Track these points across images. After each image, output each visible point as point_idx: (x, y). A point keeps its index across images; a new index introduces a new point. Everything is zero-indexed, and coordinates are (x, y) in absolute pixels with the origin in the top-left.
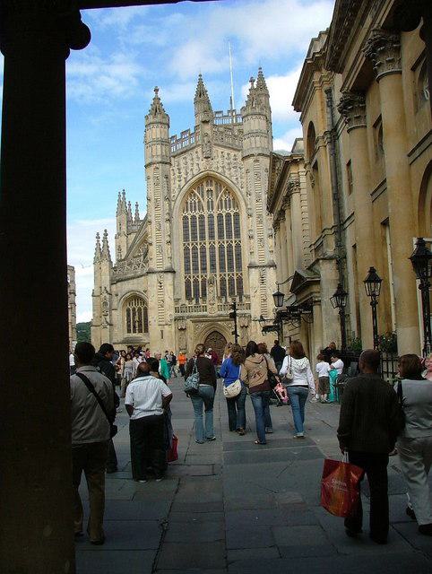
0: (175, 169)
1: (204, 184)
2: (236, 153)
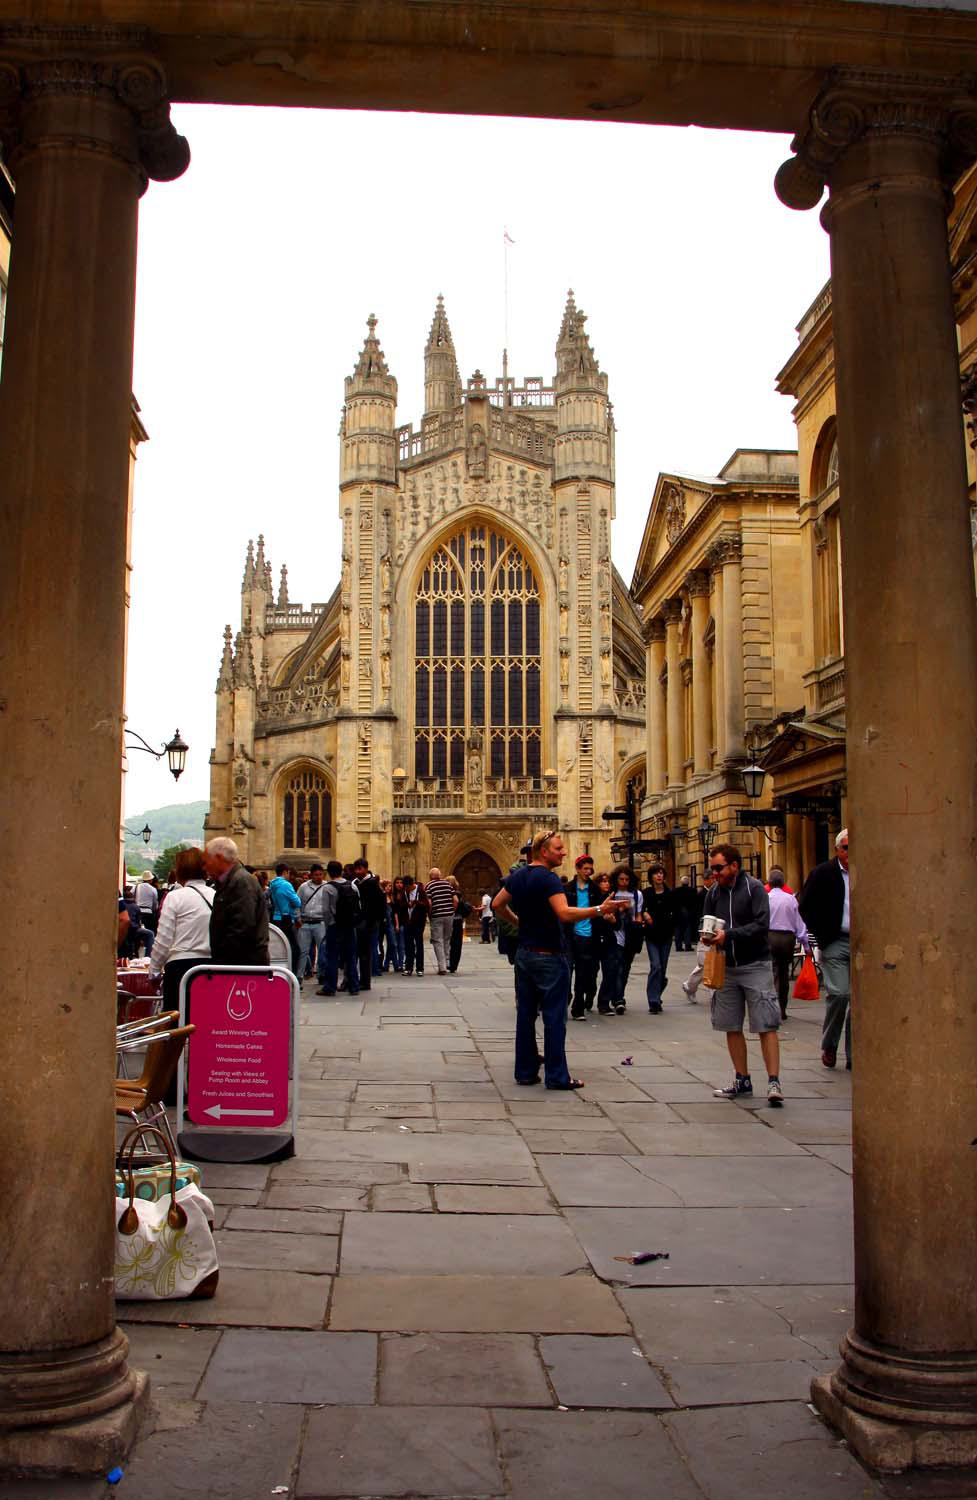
0: (407, 496)
1: (468, 535)
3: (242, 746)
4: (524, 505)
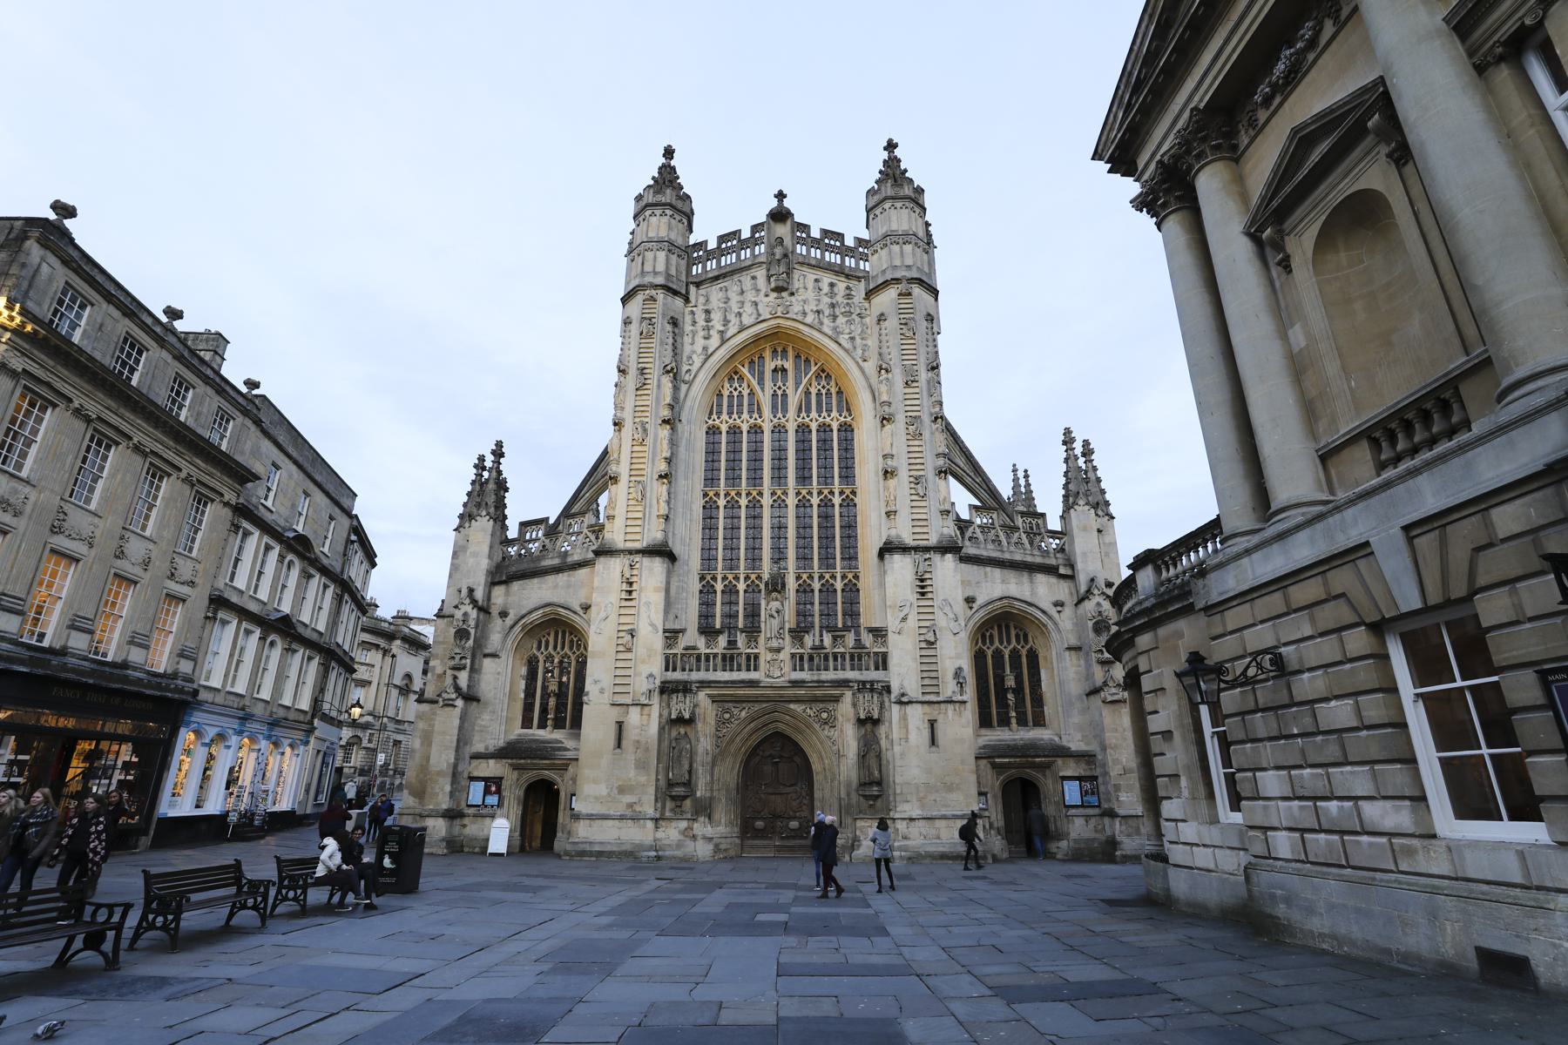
2: (853, 283)
3: (471, 591)
4: (835, 317)
